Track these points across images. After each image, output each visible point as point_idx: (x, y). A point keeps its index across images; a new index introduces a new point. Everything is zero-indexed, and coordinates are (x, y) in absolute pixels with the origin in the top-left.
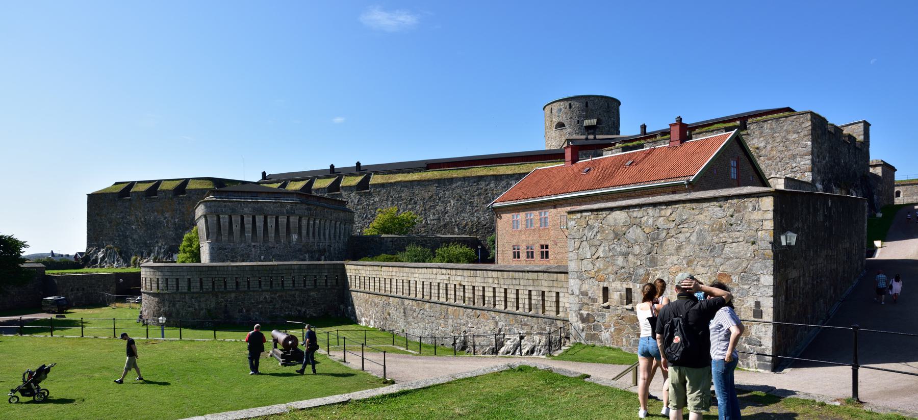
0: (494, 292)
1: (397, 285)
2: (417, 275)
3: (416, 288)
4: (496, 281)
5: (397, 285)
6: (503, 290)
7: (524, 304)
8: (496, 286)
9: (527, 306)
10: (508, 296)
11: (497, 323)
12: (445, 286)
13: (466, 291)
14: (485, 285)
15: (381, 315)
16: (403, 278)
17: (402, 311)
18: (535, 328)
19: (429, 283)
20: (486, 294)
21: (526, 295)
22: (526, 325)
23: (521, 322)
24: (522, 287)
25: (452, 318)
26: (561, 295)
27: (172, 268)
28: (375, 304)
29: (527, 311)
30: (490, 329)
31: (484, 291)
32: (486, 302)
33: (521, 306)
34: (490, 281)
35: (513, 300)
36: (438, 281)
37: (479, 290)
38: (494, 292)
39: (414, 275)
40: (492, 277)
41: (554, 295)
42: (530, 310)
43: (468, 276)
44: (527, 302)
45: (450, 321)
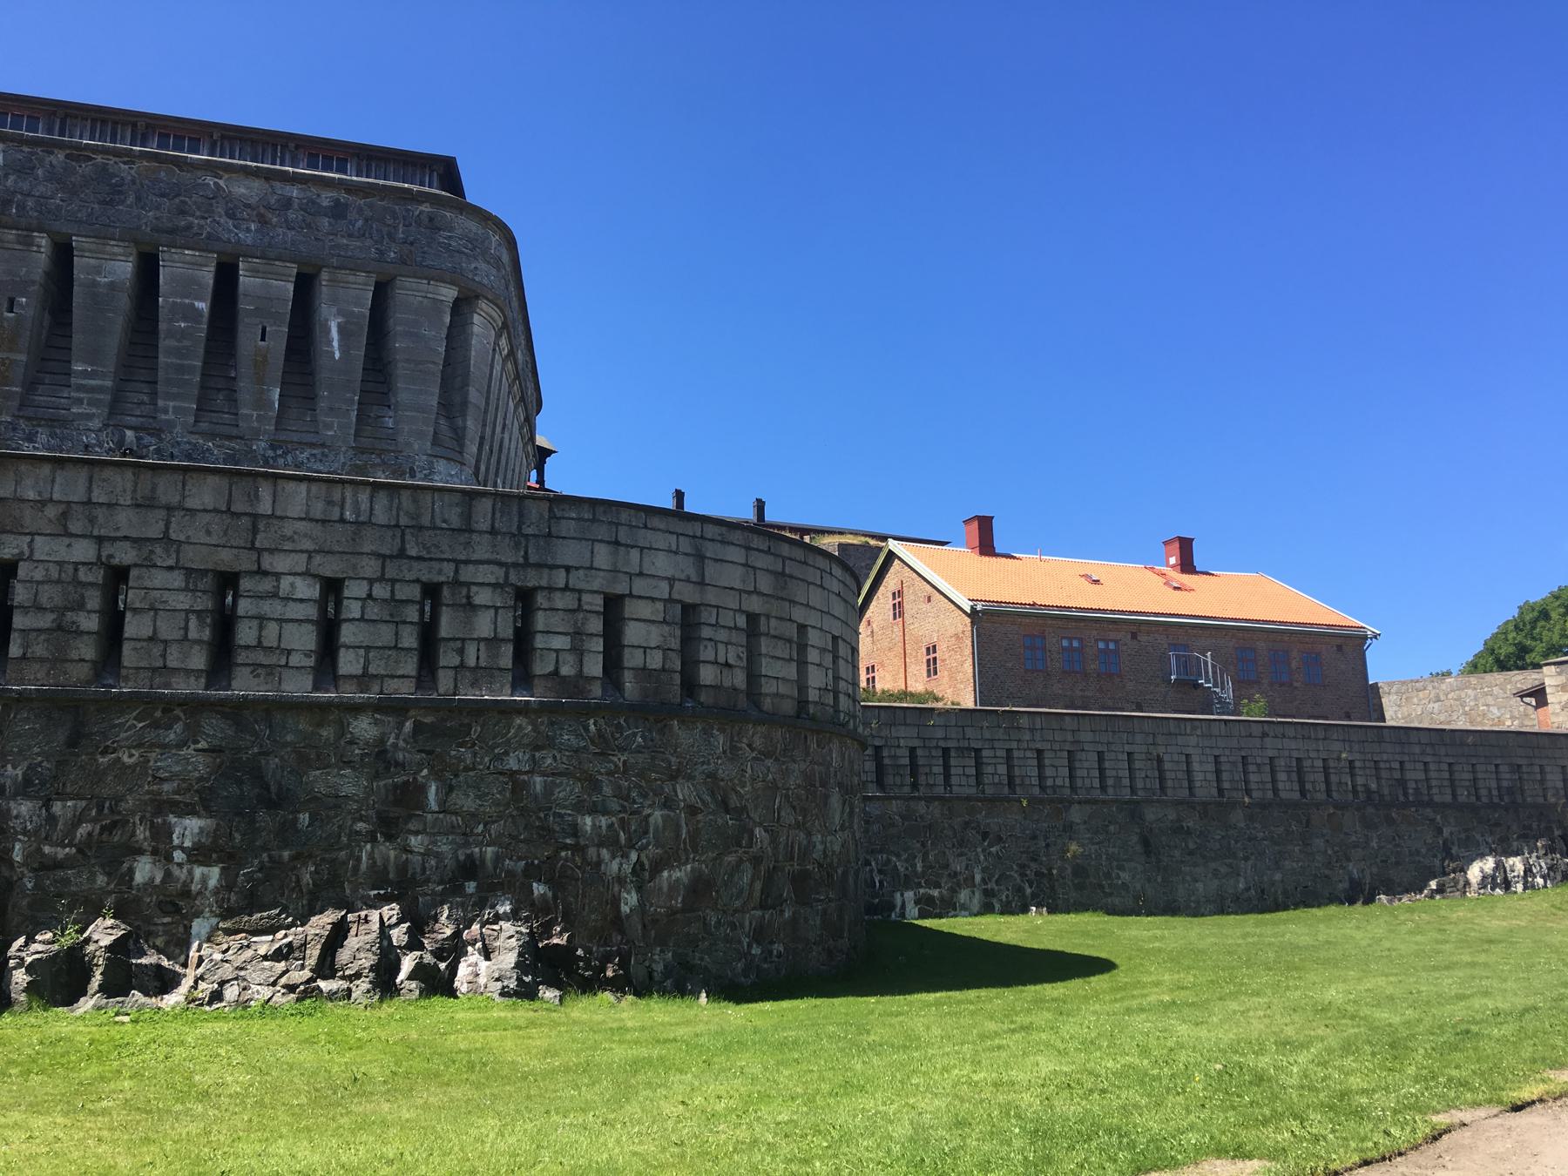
0: (1426, 771)
1: (1102, 770)
2: (1193, 740)
3: (1189, 772)
4: (1429, 750)
5: (1102, 770)
6: (1445, 767)
7: (1490, 790)
8: (1428, 759)
9: (1495, 793)
10: (1457, 776)
11: (1440, 831)
12: (1294, 764)
13: (1358, 771)
14: (1406, 758)
15: (1022, 866)
16: (1127, 748)
17: (1135, 839)
18: (1514, 828)
19: (1240, 759)
20: (1409, 775)
21: (1491, 772)
22: (1497, 824)
23: (1489, 820)
24: (1482, 760)
25: (1323, 836)
26: (1548, 769)
27: (711, 531)
28: (985, 835)
29: (1496, 800)
30: (1425, 843)
31: (1402, 769)
32: (1411, 791)
33: (1483, 792)
34: (1417, 750)
35: (1467, 783)
36: (1270, 753)
37: (1391, 769)
38: (1426, 771)
39: (1180, 740)
40: (1420, 743)
41: (1537, 769)
42: (1502, 800)
43: (1359, 742)
44: (1494, 784)
45: (1319, 843)
